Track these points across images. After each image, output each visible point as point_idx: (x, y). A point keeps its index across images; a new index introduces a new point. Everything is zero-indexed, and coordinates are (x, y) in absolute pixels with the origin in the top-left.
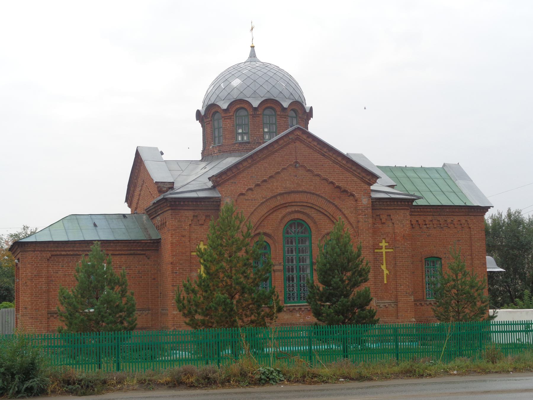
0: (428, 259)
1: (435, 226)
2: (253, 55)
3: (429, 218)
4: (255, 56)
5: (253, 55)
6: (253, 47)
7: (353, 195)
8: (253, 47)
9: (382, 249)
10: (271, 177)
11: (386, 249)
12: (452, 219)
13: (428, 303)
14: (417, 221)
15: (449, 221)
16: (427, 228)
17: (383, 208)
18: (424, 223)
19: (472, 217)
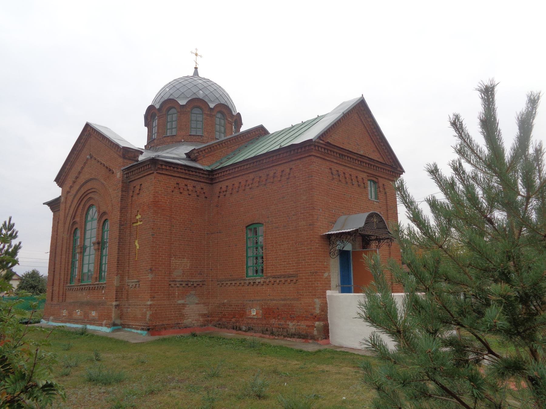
0: (250, 227)
1: (257, 185)
2: (196, 73)
3: (252, 176)
4: (198, 75)
5: (196, 73)
6: (196, 68)
7: (113, 173)
8: (196, 68)
9: (137, 222)
10: (80, 173)
11: (140, 221)
12: (275, 171)
13: (247, 282)
14: (240, 183)
15: (271, 174)
16: (250, 188)
17: (136, 178)
18: (247, 184)
19: (298, 161)
